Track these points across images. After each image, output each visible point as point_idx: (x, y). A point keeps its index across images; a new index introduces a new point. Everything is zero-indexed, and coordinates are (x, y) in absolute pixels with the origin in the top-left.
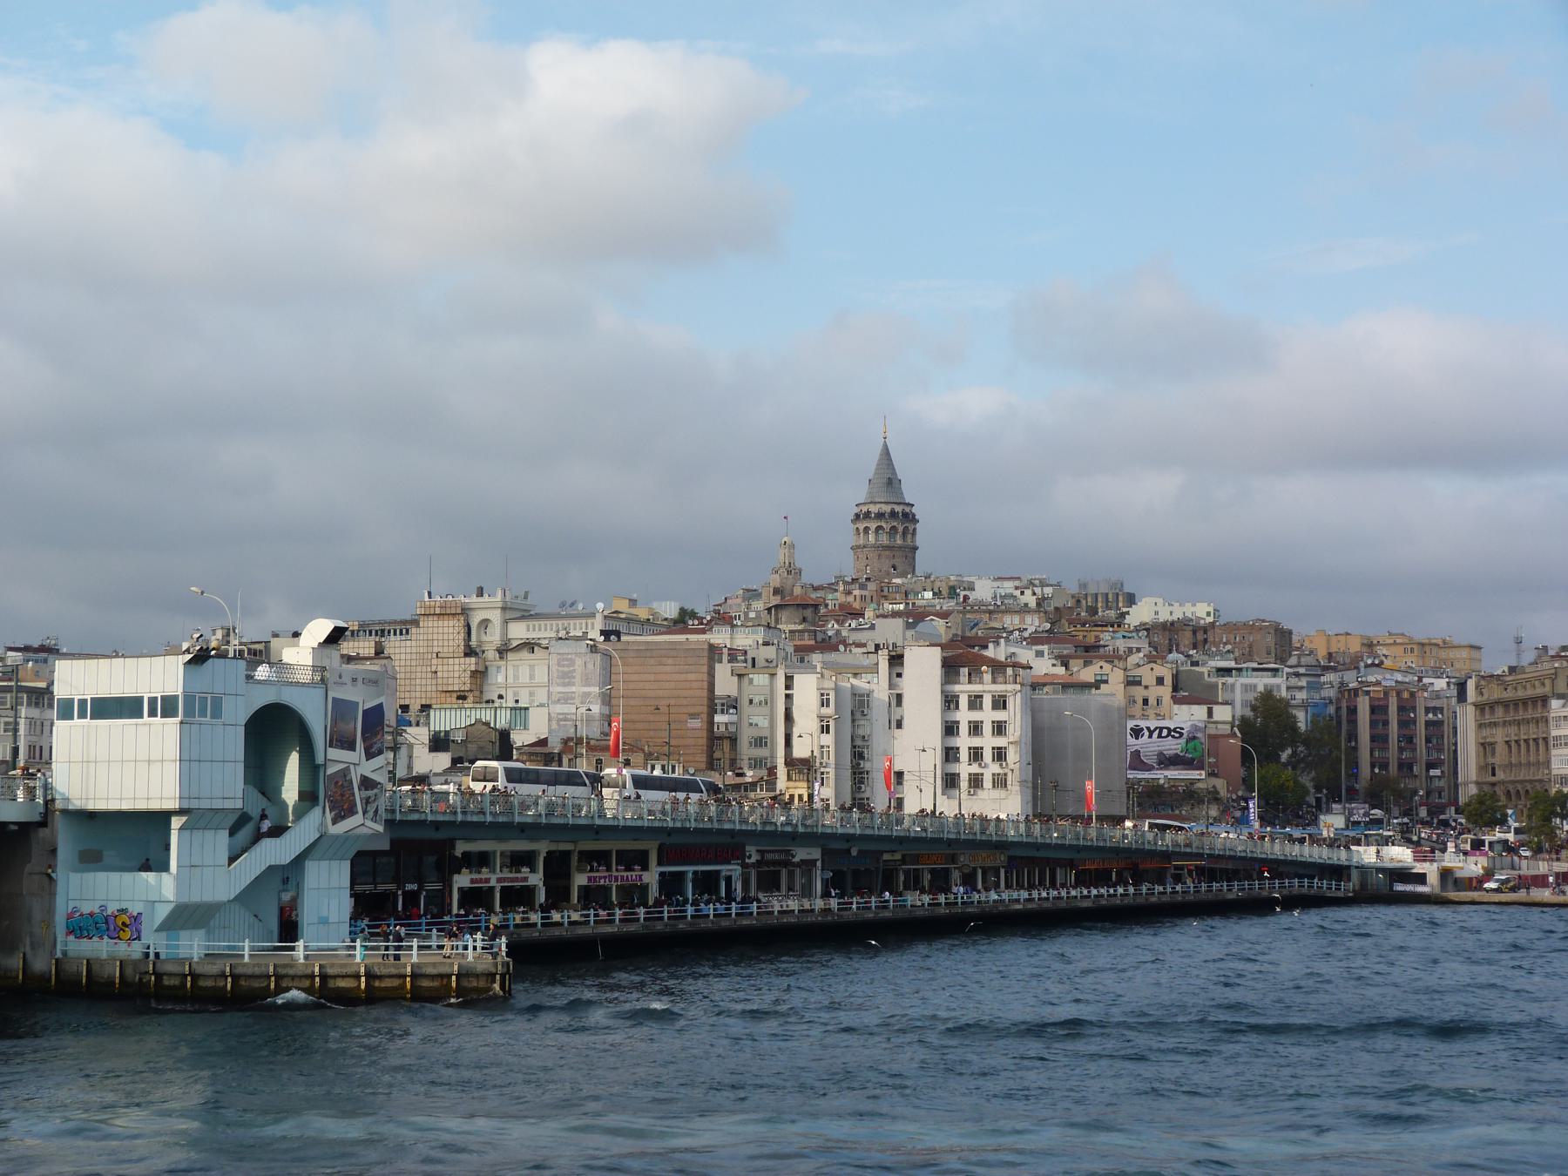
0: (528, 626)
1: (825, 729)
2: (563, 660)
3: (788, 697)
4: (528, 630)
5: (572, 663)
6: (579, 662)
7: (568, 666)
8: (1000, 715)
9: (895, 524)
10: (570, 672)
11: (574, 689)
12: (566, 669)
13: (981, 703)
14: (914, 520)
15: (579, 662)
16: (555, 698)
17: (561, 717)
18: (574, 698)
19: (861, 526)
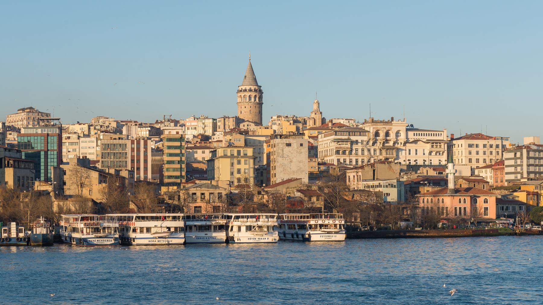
0: (414, 134)
4: (414, 135)
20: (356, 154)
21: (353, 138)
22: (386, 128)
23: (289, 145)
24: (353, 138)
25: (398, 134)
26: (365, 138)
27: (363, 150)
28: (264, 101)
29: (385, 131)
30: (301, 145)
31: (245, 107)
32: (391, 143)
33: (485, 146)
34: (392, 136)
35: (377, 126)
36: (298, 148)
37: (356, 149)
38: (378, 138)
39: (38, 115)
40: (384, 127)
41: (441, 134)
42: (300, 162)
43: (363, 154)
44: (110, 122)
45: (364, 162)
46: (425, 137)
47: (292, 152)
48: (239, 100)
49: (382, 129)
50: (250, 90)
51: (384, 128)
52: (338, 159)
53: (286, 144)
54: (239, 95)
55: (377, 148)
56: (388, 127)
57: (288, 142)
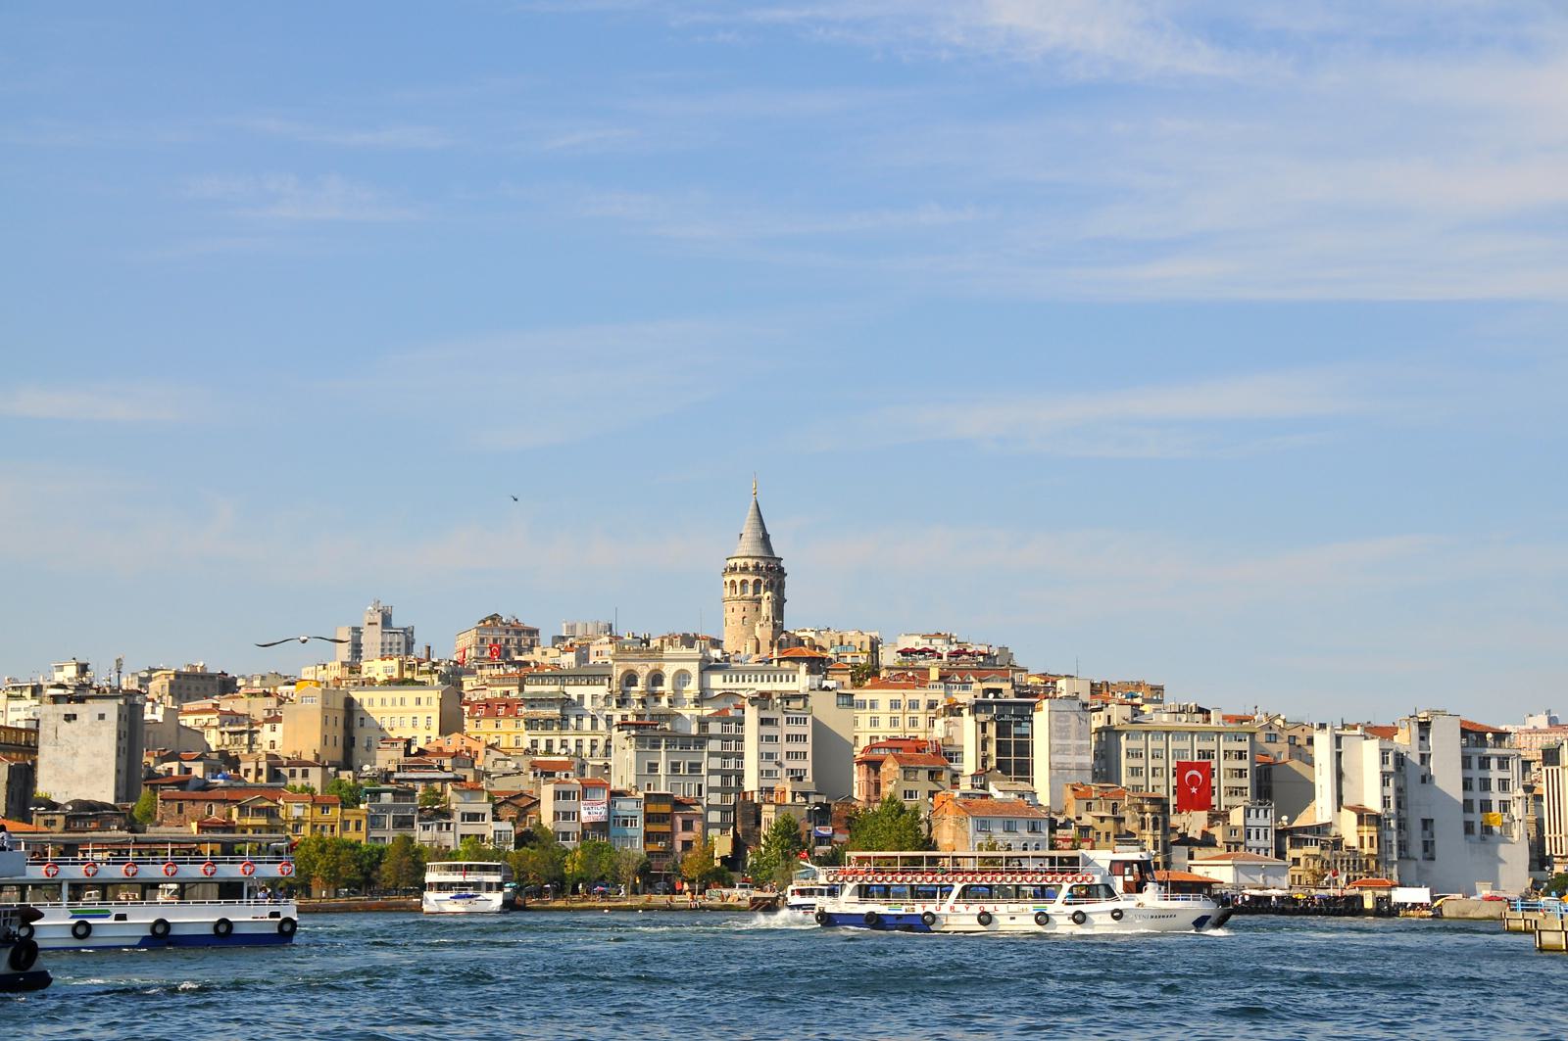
0: (725, 677)
1: (1385, 783)
2: (1061, 716)
3: (1339, 755)
4: (725, 681)
5: (1067, 719)
7: (1066, 721)
8: (1504, 775)
10: (1066, 727)
11: (1069, 742)
12: (1063, 724)
13: (1489, 762)
14: (781, 572)
18: (1069, 750)
19: (738, 579)
21: (573, 691)
23: (70, 718)
24: (573, 691)
25: (682, 677)
26: (602, 691)
28: (788, 593)
29: (646, 671)
30: (102, 717)
32: (664, 702)
33: (895, 704)
34: (667, 687)
36: (91, 724)
38: (633, 688)
41: (794, 677)
42: (95, 755)
46: (752, 685)
47: (77, 732)
48: (727, 592)
50: (757, 567)
52: (547, 741)
53: (66, 715)
54: (728, 579)
55: (629, 713)
56: (652, 665)
57: (69, 712)
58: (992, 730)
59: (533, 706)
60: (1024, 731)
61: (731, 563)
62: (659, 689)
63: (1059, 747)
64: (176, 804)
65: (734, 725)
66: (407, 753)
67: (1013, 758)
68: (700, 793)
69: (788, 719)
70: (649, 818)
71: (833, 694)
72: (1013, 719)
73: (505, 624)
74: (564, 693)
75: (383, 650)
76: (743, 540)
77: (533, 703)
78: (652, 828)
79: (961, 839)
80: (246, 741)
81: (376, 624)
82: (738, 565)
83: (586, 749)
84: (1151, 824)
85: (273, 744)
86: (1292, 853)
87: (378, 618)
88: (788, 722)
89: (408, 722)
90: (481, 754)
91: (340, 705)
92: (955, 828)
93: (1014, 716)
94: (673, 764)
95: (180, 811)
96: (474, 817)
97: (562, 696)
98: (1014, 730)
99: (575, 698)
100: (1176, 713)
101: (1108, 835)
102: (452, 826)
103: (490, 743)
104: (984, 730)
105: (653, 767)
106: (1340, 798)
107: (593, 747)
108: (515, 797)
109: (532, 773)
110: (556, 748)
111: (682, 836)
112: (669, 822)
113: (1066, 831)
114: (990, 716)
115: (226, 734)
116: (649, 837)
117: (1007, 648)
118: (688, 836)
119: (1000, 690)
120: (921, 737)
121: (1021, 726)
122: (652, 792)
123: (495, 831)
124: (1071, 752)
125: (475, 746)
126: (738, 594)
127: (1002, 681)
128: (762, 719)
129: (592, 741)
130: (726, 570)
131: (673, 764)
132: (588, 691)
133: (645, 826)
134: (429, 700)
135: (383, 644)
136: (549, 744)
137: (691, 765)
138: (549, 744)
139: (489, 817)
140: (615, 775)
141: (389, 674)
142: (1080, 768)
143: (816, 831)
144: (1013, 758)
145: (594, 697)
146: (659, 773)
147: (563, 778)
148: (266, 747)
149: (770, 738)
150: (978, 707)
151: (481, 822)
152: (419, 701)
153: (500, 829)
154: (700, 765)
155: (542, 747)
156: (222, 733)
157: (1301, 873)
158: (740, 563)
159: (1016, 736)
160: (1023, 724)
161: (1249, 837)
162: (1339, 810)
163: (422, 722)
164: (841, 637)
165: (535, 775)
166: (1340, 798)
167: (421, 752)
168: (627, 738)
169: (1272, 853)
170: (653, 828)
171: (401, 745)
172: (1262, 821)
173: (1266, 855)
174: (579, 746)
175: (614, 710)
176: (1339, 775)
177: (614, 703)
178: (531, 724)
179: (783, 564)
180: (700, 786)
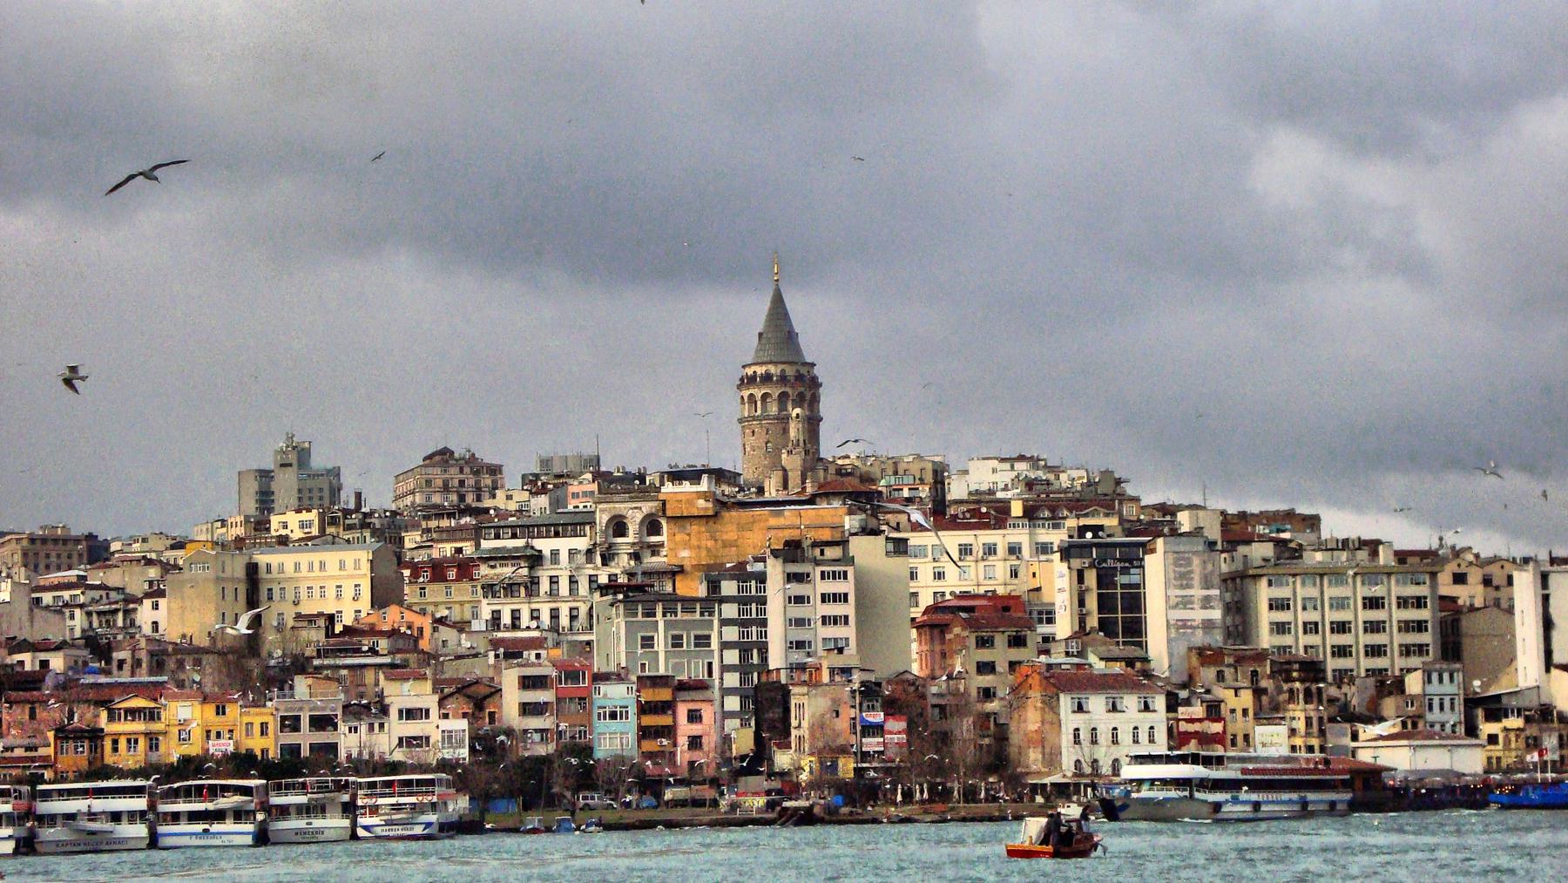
2: (1179, 559)
5: (1189, 562)
6: (1196, 561)
7: (1185, 567)
9: (802, 389)
12: (1182, 569)
14: (815, 383)
15: (1196, 561)
16: (1173, 601)
17: (1180, 623)
18: (1192, 603)
19: (758, 393)
20: (553, 594)
21: (544, 545)
22: (644, 509)
24: (544, 545)
26: (581, 543)
27: (573, 581)
28: (825, 407)
29: (639, 516)
31: (753, 432)
35: (612, 505)
37: (551, 577)
38: (620, 540)
39: (461, 471)
40: (634, 505)
43: (556, 592)
44: (510, 493)
45: (577, 616)
49: (631, 511)
50: (783, 379)
51: (636, 508)
54: (746, 394)
55: (618, 571)
58: (1091, 578)
59: (493, 567)
60: (1135, 579)
61: (750, 371)
62: (654, 539)
63: (1180, 599)
64: (28, 707)
65: (753, 583)
66: (327, 636)
67: (1120, 615)
68: (710, 673)
69: (823, 573)
70: (644, 709)
71: (881, 539)
72: (1119, 565)
73: (457, 460)
74: (532, 548)
75: (300, 499)
76: (763, 341)
77: (492, 563)
78: (649, 720)
79: (1052, 723)
80: (120, 623)
81: (290, 465)
82: (759, 373)
83: (564, 621)
84: (1301, 696)
85: (155, 624)
86: (1487, 728)
87: (292, 458)
88: (823, 577)
89: (331, 592)
90: (427, 632)
91: (240, 572)
92: (1042, 709)
93: (1120, 560)
94: (674, 637)
95: (32, 716)
96: (410, 714)
97: (529, 552)
98: (1121, 579)
99: (546, 553)
100: (1332, 550)
101: (1245, 712)
102: (386, 725)
103: (438, 615)
104: (1081, 579)
105: (648, 642)
106: (1548, 653)
107: (573, 618)
108: (470, 685)
109: (492, 654)
110: (525, 620)
111: (685, 729)
112: (670, 712)
113: (1190, 709)
114: (1087, 562)
115: (95, 616)
116: (645, 733)
117: (1112, 472)
118: (696, 729)
119: (1101, 528)
120: (1001, 591)
121: (1129, 574)
122: (647, 673)
123: (443, 731)
124: (1195, 606)
125: (418, 621)
126: (759, 412)
127: (1107, 515)
128: (789, 575)
129: (571, 609)
130: (742, 380)
131: (674, 637)
132: (564, 544)
133: (639, 718)
134: (357, 562)
135: (300, 491)
136: (515, 615)
137: (697, 637)
138: (515, 615)
139: (434, 713)
140: (598, 654)
141: (306, 530)
142: (1208, 625)
143: (862, 719)
144: (1120, 615)
145: (572, 553)
146: (656, 648)
147: (533, 658)
148: (147, 630)
149: (799, 600)
150: (1072, 550)
151: (424, 720)
152: (342, 566)
153: (450, 729)
154: (708, 637)
155: (506, 619)
156: (89, 614)
157: (1498, 754)
158: (760, 370)
159: (1123, 586)
160: (1132, 571)
161: (1431, 708)
162: (1548, 670)
163: (348, 592)
164: (896, 464)
165: (497, 656)
166: (1548, 653)
167: (348, 630)
168: (612, 605)
169: (1461, 730)
170: (649, 720)
171: (322, 622)
172: (1448, 688)
173: (1454, 732)
174: (555, 615)
175: (598, 569)
176: (1548, 624)
177: (598, 560)
178: (490, 589)
179: (816, 371)
180: (710, 664)
